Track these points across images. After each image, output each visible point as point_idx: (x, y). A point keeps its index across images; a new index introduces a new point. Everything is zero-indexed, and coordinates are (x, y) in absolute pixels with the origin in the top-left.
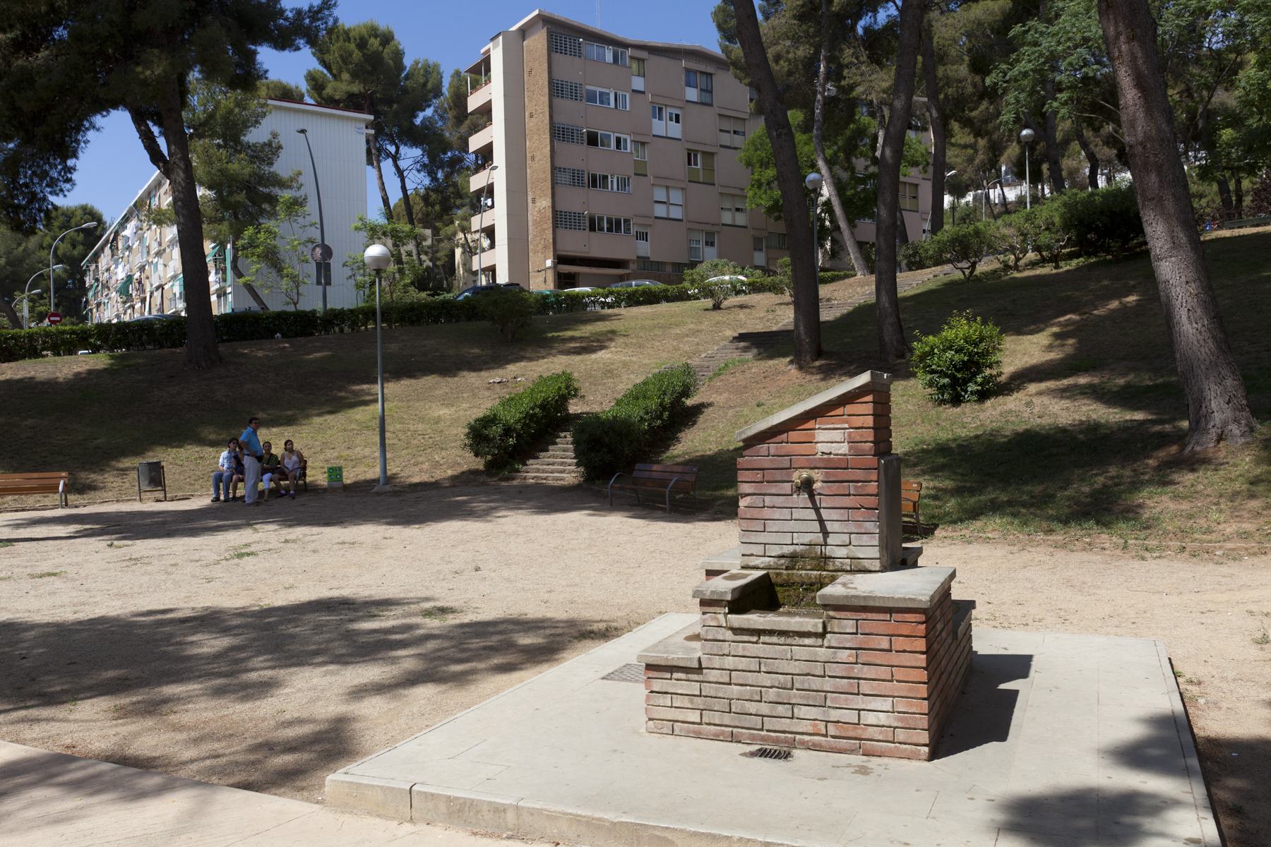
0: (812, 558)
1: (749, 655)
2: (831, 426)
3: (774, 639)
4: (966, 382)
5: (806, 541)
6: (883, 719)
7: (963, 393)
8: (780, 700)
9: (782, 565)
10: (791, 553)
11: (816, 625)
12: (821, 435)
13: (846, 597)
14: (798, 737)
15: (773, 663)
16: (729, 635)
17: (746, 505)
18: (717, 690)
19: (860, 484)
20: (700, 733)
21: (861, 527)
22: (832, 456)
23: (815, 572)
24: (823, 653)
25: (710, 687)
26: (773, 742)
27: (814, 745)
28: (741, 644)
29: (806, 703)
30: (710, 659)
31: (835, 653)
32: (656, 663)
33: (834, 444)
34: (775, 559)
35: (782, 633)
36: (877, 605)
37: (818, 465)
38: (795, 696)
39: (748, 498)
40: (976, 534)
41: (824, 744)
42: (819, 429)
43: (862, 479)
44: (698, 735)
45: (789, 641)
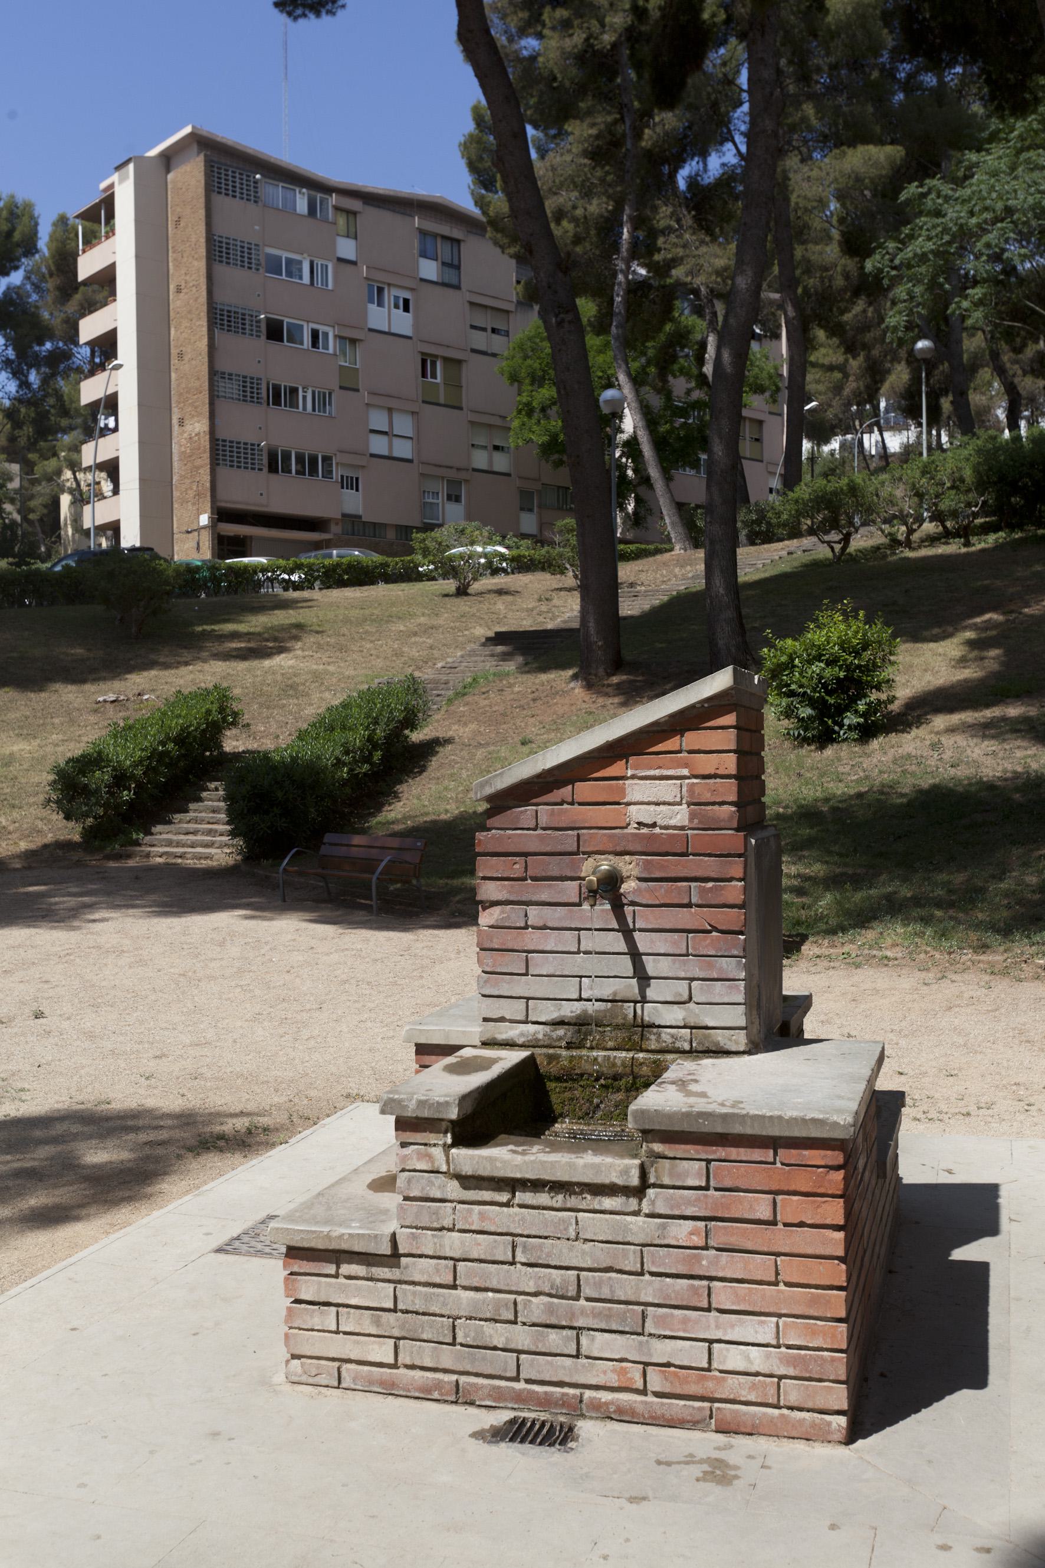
0: (617, 1027)
1: (492, 1229)
2: (657, 772)
3: (543, 1198)
4: (840, 710)
5: (606, 993)
6: (758, 1361)
7: (836, 728)
8: (553, 1321)
9: (560, 1039)
10: (578, 1017)
11: (626, 1171)
12: (636, 790)
13: (688, 1115)
14: (588, 1394)
15: (541, 1246)
16: (453, 1190)
18: (428, 1298)
19: (710, 885)
20: (393, 1385)
21: (711, 966)
22: (657, 830)
23: (624, 1054)
24: (639, 1227)
25: (414, 1293)
26: (540, 1404)
27: (620, 1410)
28: (476, 1208)
29: (603, 1326)
30: (414, 1237)
31: (664, 1227)
32: (306, 1245)
33: (662, 808)
34: (547, 1028)
35: (558, 1187)
36: (749, 1131)
37: (631, 848)
38: (583, 1312)
39: (496, 911)
40: (866, 952)
41: (640, 1409)
42: (633, 777)
43: (713, 875)
44: (390, 1390)
45: (573, 1201)
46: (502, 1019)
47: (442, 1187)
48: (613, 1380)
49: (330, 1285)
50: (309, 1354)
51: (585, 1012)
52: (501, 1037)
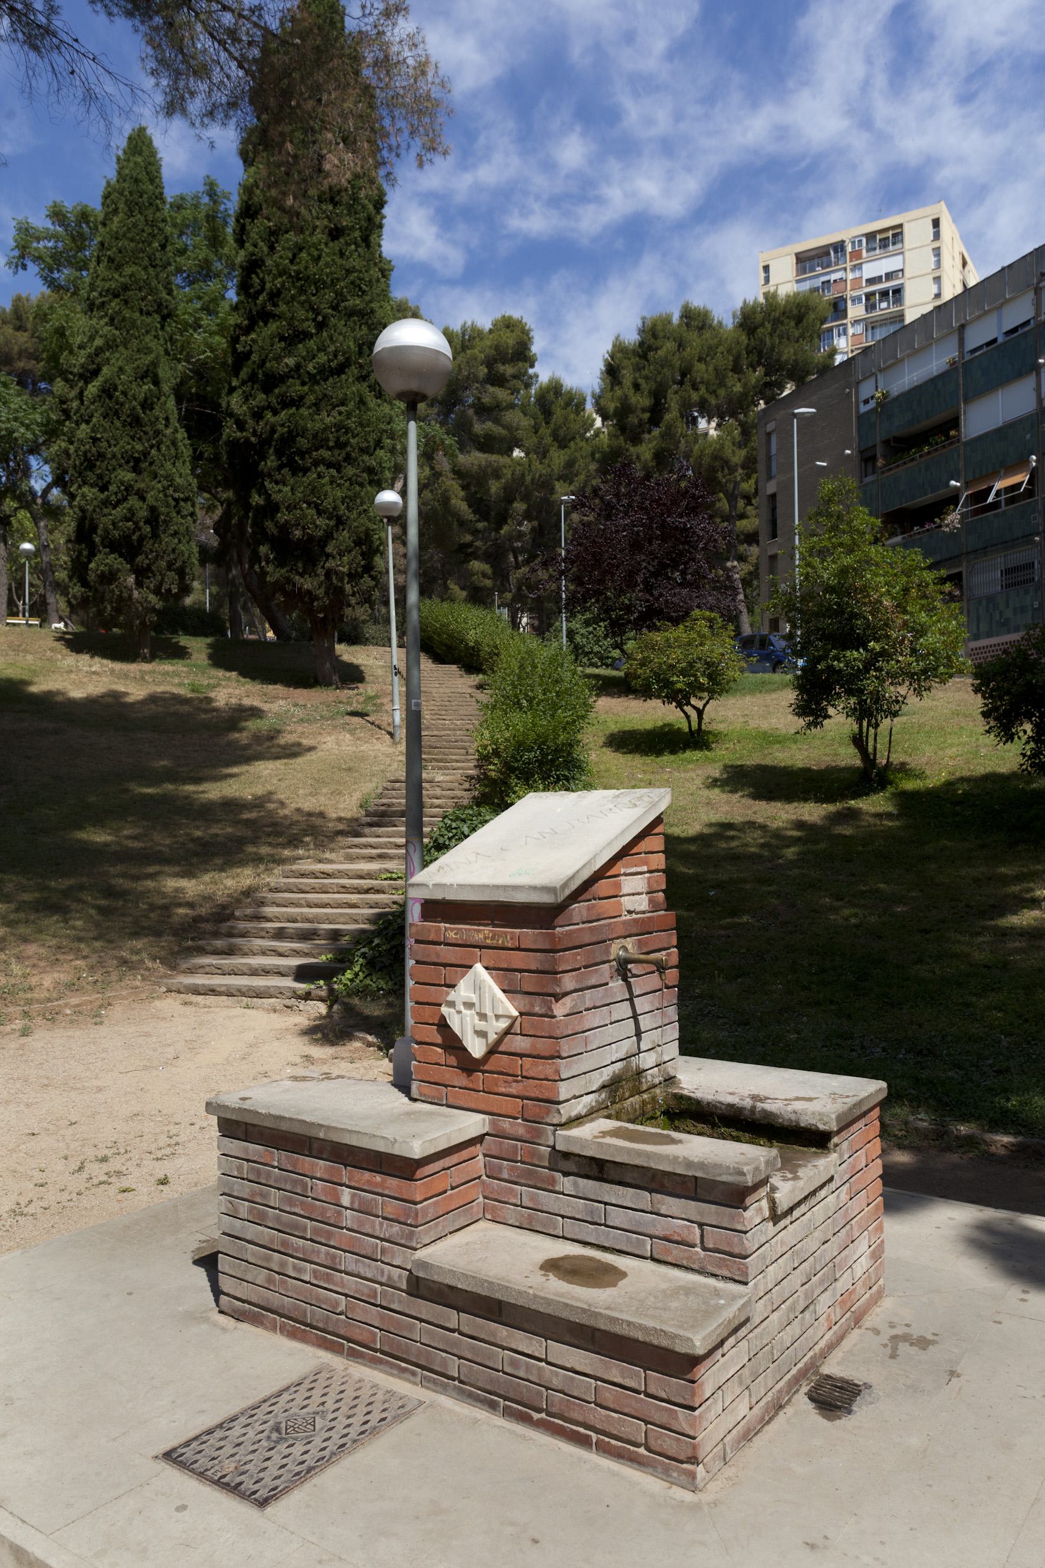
0: (627, 1080)
5: (621, 1054)
10: (611, 1079)
13: (850, 1109)
17: (567, 1012)
42: (626, 875)
43: (666, 946)
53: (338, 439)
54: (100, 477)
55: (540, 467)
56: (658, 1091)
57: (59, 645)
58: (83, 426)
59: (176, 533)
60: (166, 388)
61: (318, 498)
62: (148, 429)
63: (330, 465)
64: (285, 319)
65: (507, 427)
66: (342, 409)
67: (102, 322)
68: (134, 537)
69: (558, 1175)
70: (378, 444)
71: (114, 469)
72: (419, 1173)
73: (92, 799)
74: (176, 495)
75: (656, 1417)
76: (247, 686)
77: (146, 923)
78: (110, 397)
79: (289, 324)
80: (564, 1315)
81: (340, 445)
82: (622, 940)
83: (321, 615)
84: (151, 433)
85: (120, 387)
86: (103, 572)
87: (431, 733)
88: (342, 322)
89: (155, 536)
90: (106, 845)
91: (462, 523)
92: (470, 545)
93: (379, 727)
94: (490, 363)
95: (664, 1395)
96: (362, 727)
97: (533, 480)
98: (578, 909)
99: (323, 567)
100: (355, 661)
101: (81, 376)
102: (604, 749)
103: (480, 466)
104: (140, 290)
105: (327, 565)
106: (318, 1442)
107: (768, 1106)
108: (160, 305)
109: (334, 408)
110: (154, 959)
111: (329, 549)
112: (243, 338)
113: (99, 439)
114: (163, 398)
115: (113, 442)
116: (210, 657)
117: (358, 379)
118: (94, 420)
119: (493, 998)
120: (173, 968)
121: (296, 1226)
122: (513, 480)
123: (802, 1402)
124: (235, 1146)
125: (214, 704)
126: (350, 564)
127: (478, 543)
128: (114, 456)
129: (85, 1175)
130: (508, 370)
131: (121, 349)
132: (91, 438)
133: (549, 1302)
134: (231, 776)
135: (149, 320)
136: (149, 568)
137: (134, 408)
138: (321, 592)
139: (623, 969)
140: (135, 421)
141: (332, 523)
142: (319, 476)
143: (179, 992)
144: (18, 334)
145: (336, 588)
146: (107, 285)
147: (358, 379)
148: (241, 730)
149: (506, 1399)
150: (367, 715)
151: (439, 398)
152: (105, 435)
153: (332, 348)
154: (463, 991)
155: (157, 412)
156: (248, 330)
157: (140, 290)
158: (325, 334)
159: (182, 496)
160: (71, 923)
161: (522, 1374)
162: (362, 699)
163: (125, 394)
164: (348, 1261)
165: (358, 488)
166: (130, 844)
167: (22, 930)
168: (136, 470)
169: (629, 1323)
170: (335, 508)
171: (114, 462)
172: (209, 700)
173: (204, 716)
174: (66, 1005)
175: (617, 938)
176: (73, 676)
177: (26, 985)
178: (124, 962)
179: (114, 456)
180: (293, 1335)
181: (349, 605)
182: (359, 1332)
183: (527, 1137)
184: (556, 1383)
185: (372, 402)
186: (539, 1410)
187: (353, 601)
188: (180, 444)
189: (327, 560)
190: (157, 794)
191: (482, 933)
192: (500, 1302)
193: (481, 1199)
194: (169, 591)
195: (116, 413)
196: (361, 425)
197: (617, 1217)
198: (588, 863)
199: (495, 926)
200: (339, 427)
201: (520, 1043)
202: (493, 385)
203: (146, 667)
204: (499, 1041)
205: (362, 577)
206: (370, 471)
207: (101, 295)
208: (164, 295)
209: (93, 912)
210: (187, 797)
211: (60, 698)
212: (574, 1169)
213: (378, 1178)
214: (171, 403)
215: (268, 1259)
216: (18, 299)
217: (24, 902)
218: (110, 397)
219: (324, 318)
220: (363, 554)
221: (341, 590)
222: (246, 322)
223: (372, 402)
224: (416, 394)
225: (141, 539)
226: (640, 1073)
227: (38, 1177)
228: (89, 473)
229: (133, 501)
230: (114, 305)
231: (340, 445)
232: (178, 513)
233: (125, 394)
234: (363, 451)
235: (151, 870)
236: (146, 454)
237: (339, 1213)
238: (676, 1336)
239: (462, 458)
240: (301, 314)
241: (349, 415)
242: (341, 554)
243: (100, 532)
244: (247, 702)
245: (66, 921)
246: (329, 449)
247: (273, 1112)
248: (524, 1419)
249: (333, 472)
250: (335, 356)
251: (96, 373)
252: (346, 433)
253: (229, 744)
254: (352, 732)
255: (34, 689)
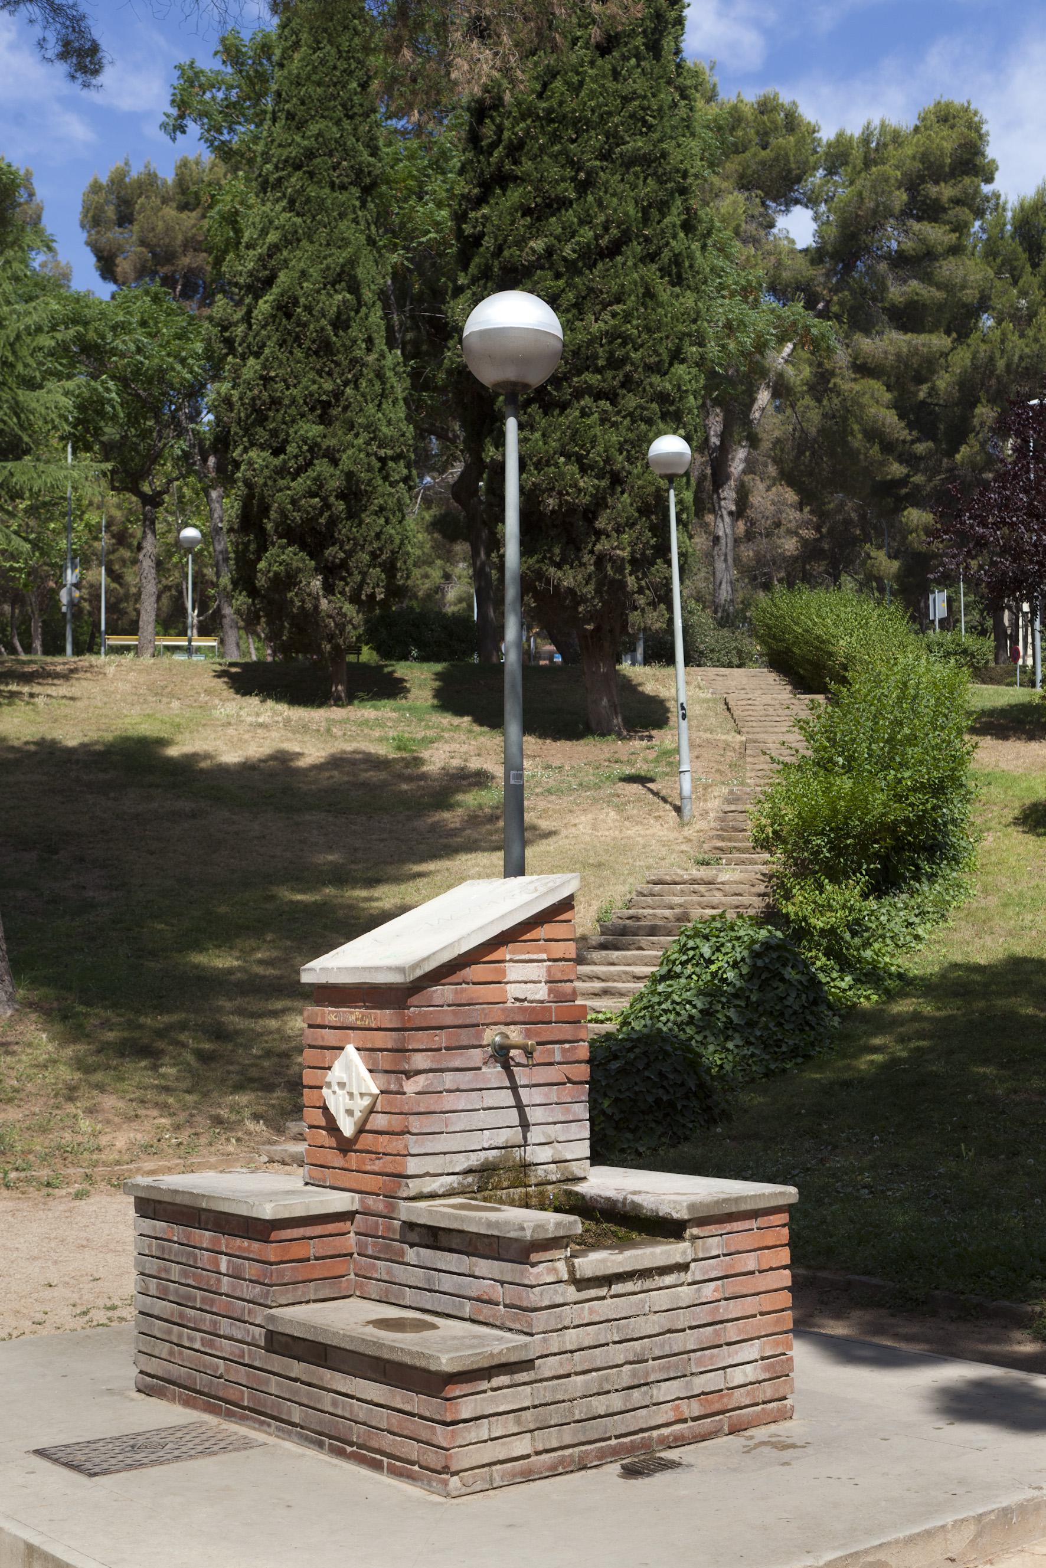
0: (509, 1169)
1: (597, 1319)
5: (500, 1141)
6: (750, 1373)
8: (636, 1382)
9: (470, 1185)
10: (482, 1165)
11: (684, 1253)
12: (514, 971)
14: (655, 1433)
15: (628, 1324)
16: (571, 1293)
17: (419, 1089)
18: (554, 1390)
19: (567, 1046)
20: (530, 1472)
21: (568, 1111)
22: (526, 1004)
23: (519, 1190)
24: (686, 1294)
25: (545, 1388)
26: (628, 1452)
27: (676, 1439)
28: (587, 1305)
29: (666, 1377)
30: (545, 1340)
31: (699, 1290)
32: (475, 1366)
33: (529, 985)
34: (460, 1177)
36: (749, 1207)
37: (517, 1019)
38: (653, 1369)
41: (687, 1433)
42: (511, 960)
43: (570, 1038)
44: (528, 1477)
45: (648, 1284)
46: (427, 1174)
47: (563, 1294)
48: (671, 1416)
49: (483, 1399)
50: (467, 1466)
51: (487, 1159)
52: (426, 1190)
53: (611, 353)
54: (274, 433)
55: (1021, 343)
56: (550, 1187)
57: (220, 684)
58: (251, 361)
59: (382, 509)
60: (368, 295)
61: (582, 447)
62: (340, 357)
63: (598, 396)
64: (531, 182)
65: (946, 287)
66: (617, 308)
67: (278, 207)
68: (322, 521)
69: (406, 1246)
70: (677, 356)
71: (293, 421)
72: (275, 1235)
73: (223, 909)
74: (382, 453)
75: (425, 1435)
76: (482, 739)
77: (254, 1073)
78: (289, 316)
79: (537, 189)
80: (361, 1349)
81: (615, 363)
82: (503, 1029)
83: (590, 627)
84: (345, 363)
85: (302, 300)
86: (276, 574)
87: (740, 808)
88: (618, 177)
89: (353, 515)
90: (230, 971)
91: (888, 447)
92: (904, 481)
93: (665, 800)
94: (913, 185)
95: (428, 1414)
96: (639, 800)
97: (1008, 366)
98: (443, 993)
99: (592, 552)
100: (663, 693)
101: (249, 288)
102: (1010, 830)
103: (898, 355)
104: (331, 155)
105: (598, 547)
106: (161, 1454)
107: (637, 1199)
108: (359, 173)
109: (604, 309)
110: (256, 1117)
111: (600, 523)
112: (472, 214)
113: (272, 379)
114: (364, 309)
115: (292, 381)
116: (438, 694)
117: (642, 260)
118: (267, 351)
119: (358, 1074)
120: (280, 1130)
121: (190, 1297)
122: (975, 367)
123: (616, 1468)
124: (149, 1225)
125: (425, 769)
126: (633, 544)
127: (918, 479)
128: (293, 401)
129: (87, 1318)
130: (945, 191)
131: (304, 243)
132: (262, 377)
133: (352, 1339)
134: (421, 875)
135: (342, 197)
136: (344, 565)
137: (323, 329)
138: (589, 590)
139: (501, 1055)
140: (325, 348)
141: (604, 483)
142: (584, 414)
143: (284, 1163)
144: (184, 215)
145: (613, 581)
146: (285, 153)
147: (642, 260)
148: (450, 807)
149: (330, 1437)
150: (652, 780)
151: (829, 248)
152: (281, 372)
153: (601, 218)
154: (337, 1073)
155: (354, 332)
156: (480, 201)
157: (331, 155)
158: (590, 198)
159: (390, 452)
160: (163, 1070)
161: (339, 1412)
162: (652, 755)
163: (308, 309)
164: (225, 1326)
165: (643, 427)
166: (260, 970)
167: (98, 1077)
168: (325, 420)
169: (402, 1350)
170: (608, 461)
171: (293, 411)
172: (418, 761)
173: (405, 787)
174: (138, 1170)
175: (495, 1024)
176: (231, 731)
177: (93, 1143)
178: (218, 1121)
179: (293, 401)
180: (187, 1403)
181: (636, 608)
182: (232, 1393)
183: (385, 1212)
184: (362, 1417)
185: (664, 291)
186: (351, 1444)
187: (641, 601)
188: (389, 374)
189: (598, 540)
190: (315, 903)
191: (353, 1015)
192: (325, 1346)
193: (352, 1276)
194: (372, 596)
195: (297, 338)
196: (649, 330)
197: (447, 1283)
198: (451, 945)
199: (368, 1008)
200: (612, 336)
201: (379, 1121)
202: (919, 219)
203: (336, 713)
204: (366, 1121)
205: (653, 563)
206: (663, 398)
207: (276, 168)
208: (366, 157)
209: (190, 1058)
210: (351, 907)
211: (204, 765)
212: (417, 1240)
213: (246, 1243)
214: (376, 316)
215: (169, 1332)
216: (184, 164)
217: (108, 1043)
218: (289, 316)
219: (589, 174)
220: (653, 528)
221: (622, 584)
222: (476, 191)
223: (664, 291)
224: (514, 384)
225: (333, 522)
226: (526, 1166)
227: (39, 1317)
228: (259, 429)
229: (322, 467)
230: (295, 180)
231: (615, 363)
232: (386, 478)
233: (308, 309)
234: (650, 369)
235: (279, 1005)
236: (337, 395)
237: (219, 1280)
238: (431, 1356)
239: (866, 344)
240: (555, 172)
241: (627, 317)
242: (619, 530)
243: (273, 515)
244: (474, 765)
245: (155, 1068)
246: (598, 370)
247: (172, 1187)
248: (340, 1453)
249: (604, 404)
250: (606, 229)
251: (269, 282)
252: (624, 344)
253: (434, 828)
254: (620, 809)
255: (173, 752)
